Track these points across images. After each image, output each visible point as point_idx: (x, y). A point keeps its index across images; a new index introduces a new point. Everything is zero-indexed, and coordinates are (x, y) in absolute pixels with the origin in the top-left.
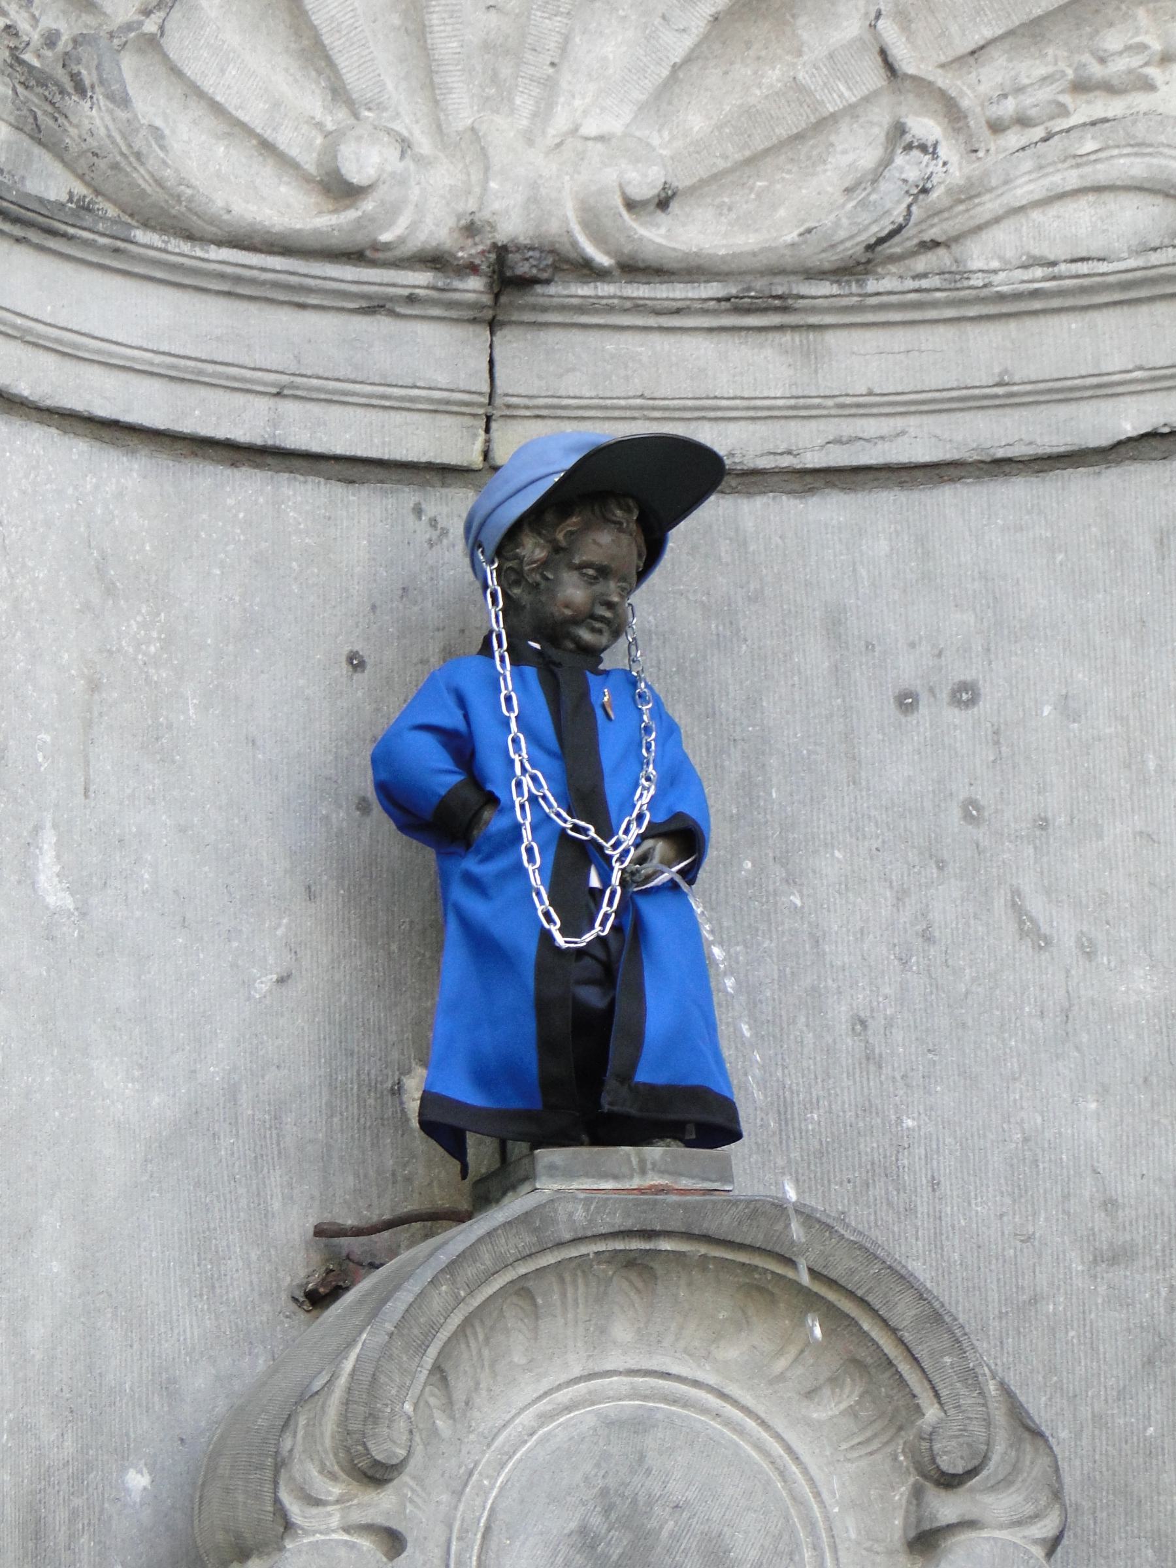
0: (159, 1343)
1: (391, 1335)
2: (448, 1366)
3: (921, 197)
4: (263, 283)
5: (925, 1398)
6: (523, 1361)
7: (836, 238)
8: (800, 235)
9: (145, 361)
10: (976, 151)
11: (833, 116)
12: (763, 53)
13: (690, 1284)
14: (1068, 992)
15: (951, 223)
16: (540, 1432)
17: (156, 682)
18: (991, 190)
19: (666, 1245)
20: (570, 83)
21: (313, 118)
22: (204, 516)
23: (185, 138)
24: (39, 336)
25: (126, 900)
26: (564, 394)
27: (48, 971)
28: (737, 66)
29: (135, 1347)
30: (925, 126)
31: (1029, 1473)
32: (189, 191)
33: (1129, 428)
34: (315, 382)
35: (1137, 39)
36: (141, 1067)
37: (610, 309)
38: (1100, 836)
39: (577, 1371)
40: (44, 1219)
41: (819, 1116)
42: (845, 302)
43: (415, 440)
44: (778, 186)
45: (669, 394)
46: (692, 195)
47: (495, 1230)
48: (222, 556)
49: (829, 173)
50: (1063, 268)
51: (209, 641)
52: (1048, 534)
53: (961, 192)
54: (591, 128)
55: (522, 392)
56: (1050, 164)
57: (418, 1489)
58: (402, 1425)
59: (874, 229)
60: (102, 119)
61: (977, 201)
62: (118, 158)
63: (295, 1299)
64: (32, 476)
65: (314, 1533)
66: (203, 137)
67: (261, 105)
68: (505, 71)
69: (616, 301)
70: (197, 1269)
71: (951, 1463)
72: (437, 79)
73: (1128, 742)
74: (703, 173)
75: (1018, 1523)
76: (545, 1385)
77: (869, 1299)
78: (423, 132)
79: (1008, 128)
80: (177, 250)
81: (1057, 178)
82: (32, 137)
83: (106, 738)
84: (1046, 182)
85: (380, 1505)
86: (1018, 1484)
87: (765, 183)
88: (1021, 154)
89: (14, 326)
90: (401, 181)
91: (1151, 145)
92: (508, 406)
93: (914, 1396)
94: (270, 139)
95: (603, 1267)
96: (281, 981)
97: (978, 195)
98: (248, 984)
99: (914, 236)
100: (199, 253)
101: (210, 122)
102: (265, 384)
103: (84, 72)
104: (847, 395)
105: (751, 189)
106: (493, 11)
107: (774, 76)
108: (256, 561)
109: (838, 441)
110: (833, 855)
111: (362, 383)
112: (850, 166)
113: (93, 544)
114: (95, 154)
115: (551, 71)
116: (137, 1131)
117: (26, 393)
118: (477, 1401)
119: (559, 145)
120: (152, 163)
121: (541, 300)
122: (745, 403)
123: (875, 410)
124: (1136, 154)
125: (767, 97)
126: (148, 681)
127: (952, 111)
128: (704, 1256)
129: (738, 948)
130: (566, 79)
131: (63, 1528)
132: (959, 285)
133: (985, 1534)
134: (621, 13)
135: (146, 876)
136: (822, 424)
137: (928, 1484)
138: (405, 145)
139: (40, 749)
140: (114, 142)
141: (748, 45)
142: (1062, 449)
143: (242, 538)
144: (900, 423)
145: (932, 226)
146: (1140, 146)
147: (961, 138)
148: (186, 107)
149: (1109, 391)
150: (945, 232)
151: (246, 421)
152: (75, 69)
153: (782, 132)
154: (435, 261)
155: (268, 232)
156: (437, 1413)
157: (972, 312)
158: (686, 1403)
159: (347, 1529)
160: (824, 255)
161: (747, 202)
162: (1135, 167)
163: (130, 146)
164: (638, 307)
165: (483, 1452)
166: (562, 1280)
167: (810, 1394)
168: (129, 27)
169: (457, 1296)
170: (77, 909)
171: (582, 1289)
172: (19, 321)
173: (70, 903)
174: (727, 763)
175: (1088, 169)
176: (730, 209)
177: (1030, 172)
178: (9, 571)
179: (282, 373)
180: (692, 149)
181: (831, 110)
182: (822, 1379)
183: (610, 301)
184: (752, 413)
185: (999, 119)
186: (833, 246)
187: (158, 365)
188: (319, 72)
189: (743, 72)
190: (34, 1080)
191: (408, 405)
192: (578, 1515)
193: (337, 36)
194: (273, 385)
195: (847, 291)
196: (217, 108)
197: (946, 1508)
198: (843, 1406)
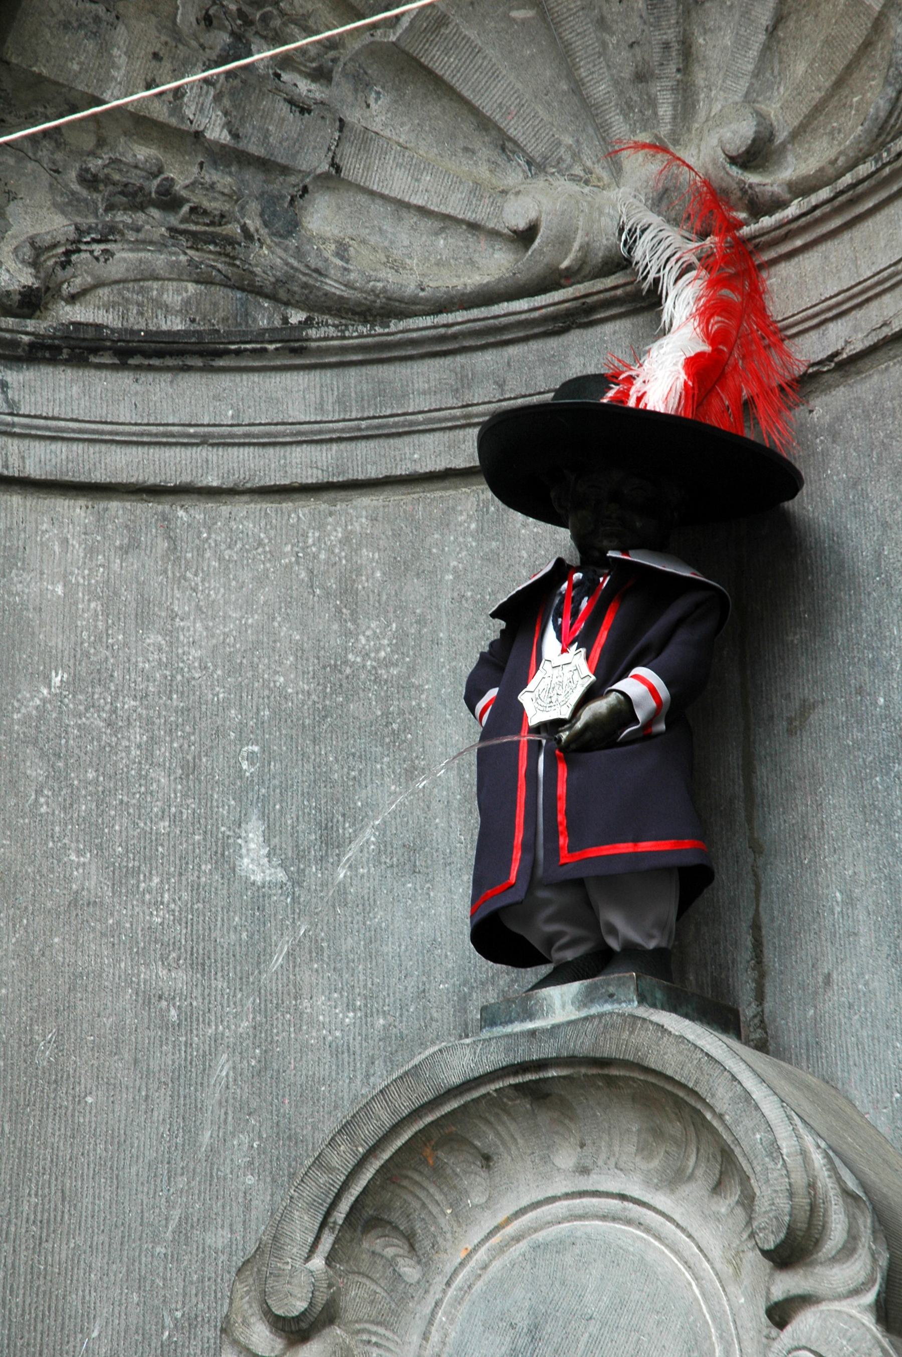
2: (394, 1216)
4: (454, 337)
11: (881, 13)
17: (386, 681)
19: (553, 1073)
20: (705, 80)
22: (436, 536)
23: (407, 243)
24: (222, 436)
32: (380, 285)
39: (525, 1202)
46: (805, 132)
48: (454, 563)
51: (441, 635)
62: (304, 279)
74: (805, 109)
94: (472, 220)
101: (428, 224)
105: (851, 106)
106: (635, 45)
108: (489, 560)
115: (679, 76)
116: (358, 1052)
117: (215, 484)
126: (377, 680)
128: (585, 1075)
130: (700, 77)
133: (824, 1307)
140: (292, 267)
143: (474, 544)
148: (400, 219)
153: (853, 46)
155: (463, 294)
163: (307, 266)
165: (444, 1292)
166: (487, 1122)
171: (513, 1127)
172: (192, 430)
173: (281, 876)
176: (840, 131)
179: (490, 402)
180: (795, 92)
187: (367, 428)
192: (508, 1339)
196: (423, 211)
197: (786, 1284)
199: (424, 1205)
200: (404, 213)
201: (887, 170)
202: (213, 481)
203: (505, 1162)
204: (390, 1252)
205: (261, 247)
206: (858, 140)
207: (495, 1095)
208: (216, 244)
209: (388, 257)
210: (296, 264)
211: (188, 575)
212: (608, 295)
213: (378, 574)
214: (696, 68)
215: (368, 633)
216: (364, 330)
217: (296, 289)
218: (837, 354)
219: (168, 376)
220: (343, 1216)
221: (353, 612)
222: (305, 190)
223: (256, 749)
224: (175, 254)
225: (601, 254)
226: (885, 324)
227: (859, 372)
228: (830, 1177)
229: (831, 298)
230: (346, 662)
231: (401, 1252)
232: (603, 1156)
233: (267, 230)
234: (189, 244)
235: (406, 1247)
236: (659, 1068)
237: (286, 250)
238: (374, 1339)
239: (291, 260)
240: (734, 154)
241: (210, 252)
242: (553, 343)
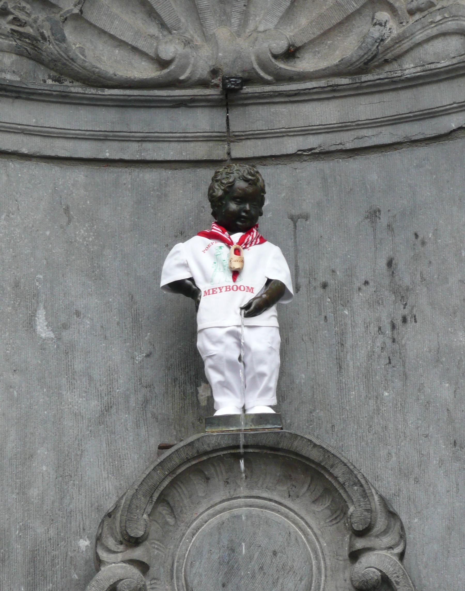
0: (94, 492)
1: (137, 490)
2: (169, 499)
3: (382, 43)
4: (130, 101)
6: (203, 495)
7: (352, 62)
8: (339, 62)
9: (81, 135)
10: (402, 23)
14: (438, 342)
15: (395, 51)
16: (209, 521)
18: (407, 38)
20: (254, 11)
21: (154, 35)
23: (101, 48)
24: (30, 131)
25: (79, 332)
26: (256, 129)
27: (42, 361)
29: (83, 494)
31: (394, 528)
32: (97, 70)
33: (454, 126)
34: (156, 134)
36: (86, 392)
37: (271, 96)
38: (448, 283)
40: (39, 451)
41: (355, 393)
42: (355, 86)
43: (200, 151)
44: (336, 42)
45: (295, 126)
47: (179, 449)
49: (354, 36)
54: (261, 28)
55: (240, 130)
56: (426, 26)
57: (161, 545)
59: (366, 56)
60: (54, 48)
61: (403, 42)
62: (65, 61)
64: (33, 181)
65: (111, 564)
66: (109, 48)
67: (130, 34)
68: (228, 10)
69: (272, 93)
70: (111, 464)
72: (201, 16)
76: (212, 503)
77: (326, 466)
78: (198, 36)
80: (90, 93)
81: (429, 31)
82: (28, 58)
83: (69, 273)
85: (138, 553)
86: (390, 533)
88: (416, 23)
89: (18, 129)
90: (186, 56)
91: (457, 16)
92: (236, 136)
93: (346, 502)
96: (148, 356)
97: (403, 40)
98: (133, 358)
99: (382, 58)
103: (45, 32)
104: (359, 121)
105: (326, 44)
109: (358, 138)
110: (359, 294)
111: (175, 133)
112: (360, 32)
113: (63, 203)
114: (56, 61)
115: (244, 8)
116: (84, 416)
117: (26, 152)
118: (185, 511)
120: (79, 62)
121: (243, 96)
122: (324, 127)
123: (370, 126)
124: (454, 20)
125: (327, 9)
129: (326, 332)
130: (252, 10)
131: (48, 563)
132: (393, 76)
133: (376, 552)
136: (352, 133)
138: (187, 43)
139: (37, 281)
140: (61, 56)
142: (433, 135)
144: (379, 129)
145: (388, 53)
146: (454, 17)
150: (393, 55)
151: (131, 151)
152: (41, 31)
153: (334, 22)
154: (204, 84)
155: (133, 81)
156: (167, 516)
157: (399, 86)
158: (266, 508)
159: (124, 562)
160: (350, 68)
161: (325, 50)
162: (451, 25)
163: (68, 56)
164: (280, 94)
166: (214, 465)
167: (314, 502)
168: (68, 12)
170: (56, 337)
172: (19, 127)
173: (52, 335)
174: (321, 262)
175: (440, 27)
176: (319, 53)
177: (420, 30)
178: (21, 217)
180: (301, 32)
181: (351, 12)
183: (269, 93)
184: (326, 130)
185: (411, 9)
186: (351, 65)
188: (155, 19)
190: (34, 402)
193: (159, 4)
195: (354, 82)
196: (112, 37)
197: (360, 544)
198: (326, 506)
199: (180, 495)
202: (25, 151)
204: (164, 512)
205: (50, 44)
207: (222, 456)
208: (29, 39)
209: (94, 54)
210: (63, 54)
211: (14, 193)
215: (84, 229)
219: (11, 100)
220: (156, 498)
222: (66, 19)
223: (41, 277)
224: (11, 41)
225: (198, 76)
226: (341, 144)
228: (379, 505)
231: (168, 512)
232: (260, 483)
233: (53, 37)
234: (18, 37)
235: (170, 511)
236: (307, 455)
237: (60, 48)
238: (156, 546)
239: (61, 53)
241: (26, 42)
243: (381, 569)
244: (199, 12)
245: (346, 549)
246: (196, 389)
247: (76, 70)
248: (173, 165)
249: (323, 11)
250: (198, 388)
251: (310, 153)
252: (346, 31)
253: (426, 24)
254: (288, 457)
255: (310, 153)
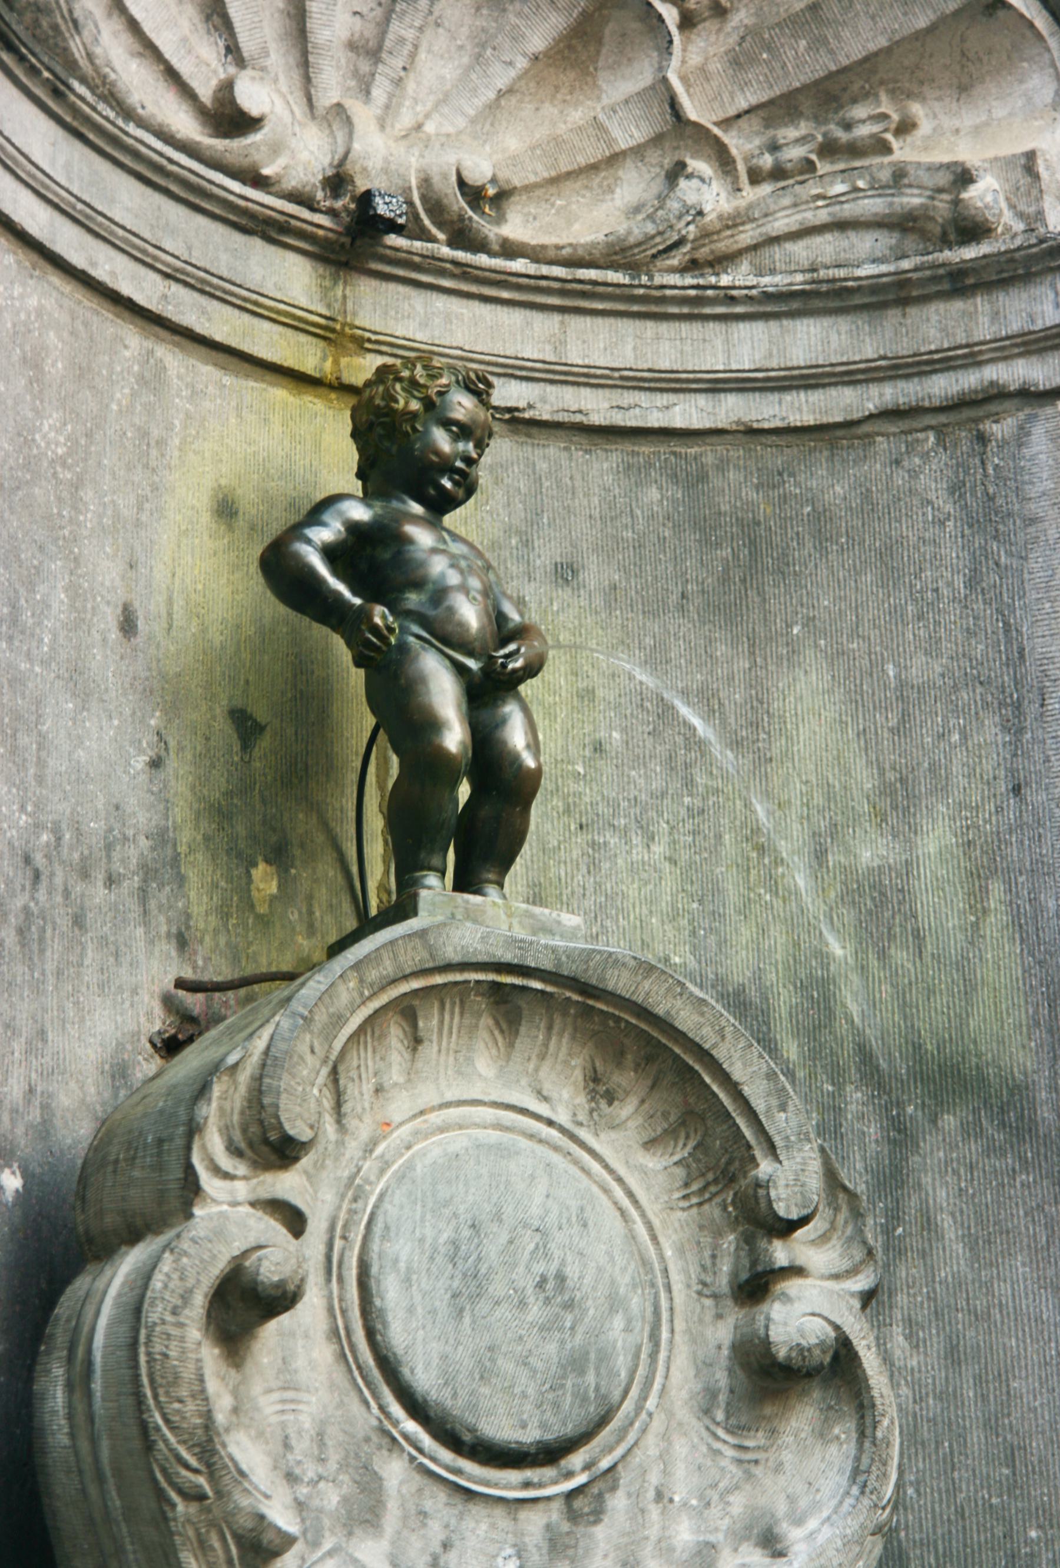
3: (698, 218)
4: (167, 174)
5: (758, 1153)
6: (401, 1080)
7: (627, 244)
11: (623, 153)
12: (568, 97)
13: (550, 1028)
19: (537, 985)
28: (547, 105)
30: (699, 165)
35: (879, 110)
37: (442, 273)
39: (449, 1096)
44: (574, 207)
50: (822, 274)
52: (798, 491)
53: (728, 219)
58: (313, 1100)
61: (741, 228)
63: (154, 1045)
69: (448, 266)
71: (786, 1208)
72: (311, 58)
73: (870, 654)
75: (836, 1277)
77: (714, 1052)
79: (764, 180)
81: (809, 215)
84: (798, 217)
87: (564, 203)
88: (780, 192)
95: (479, 999)
96: (156, 764)
97: (743, 224)
100: (120, 122)
102: (164, 263)
105: (553, 205)
107: (577, 116)
111: (240, 286)
114: (39, 10)
115: (402, 74)
119: (405, 137)
121: (388, 252)
122: (547, 366)
124: (880, 196)
127: (724, 159)
133: (808, 1281)
134: (459, 42)
135: (46, 640)
137: (760, 1232)
141: (557, 88)
144: (672, 398)
145: (704, 245)
147: (729, 179)
149: (853, 378)
150: (712, 252)
153: (582, 161)
159: (253, 1204)
160: (615, 258)
163: (70, 12)
164: (464, 272)
167: (649, 1144)
169: (362, 994)
175: (837, 208)
176: (535, 218)
179: (177, 258)
182: (659, 1131)
186: (623, 250)
187: (80, 212)
189: (549, 110)
191: (274, 316)
194: (168, 265)
195: (636, 282)
198: (676, 1158)
200: (116, 13)
201: (641, 291)
203: (429, 1050)
206: (594, 245)
212: (310, 228)
213: (60, 365)
214: (412, 75)
216: (112, 115)
217: (45, 24)
218: (517, 409)
221: (41, 391)
225: (293, 183)
226: (580, 412)
227: (529, 436)
229: (528, 360)
230: (33, 440)
240: (470, 182)
242: (238, 238)
243: (839, 1322)
244: (310, 49)
245: (725, 1268)
246: (248, 873)
247: (73, 54)
248: (221, 357)
249: (562, 128)
250: (253, 872)
251: (507, 416)
252: (600, 186)
253: (804, 198)
254: (618, 1019)
255: (507, 416)
